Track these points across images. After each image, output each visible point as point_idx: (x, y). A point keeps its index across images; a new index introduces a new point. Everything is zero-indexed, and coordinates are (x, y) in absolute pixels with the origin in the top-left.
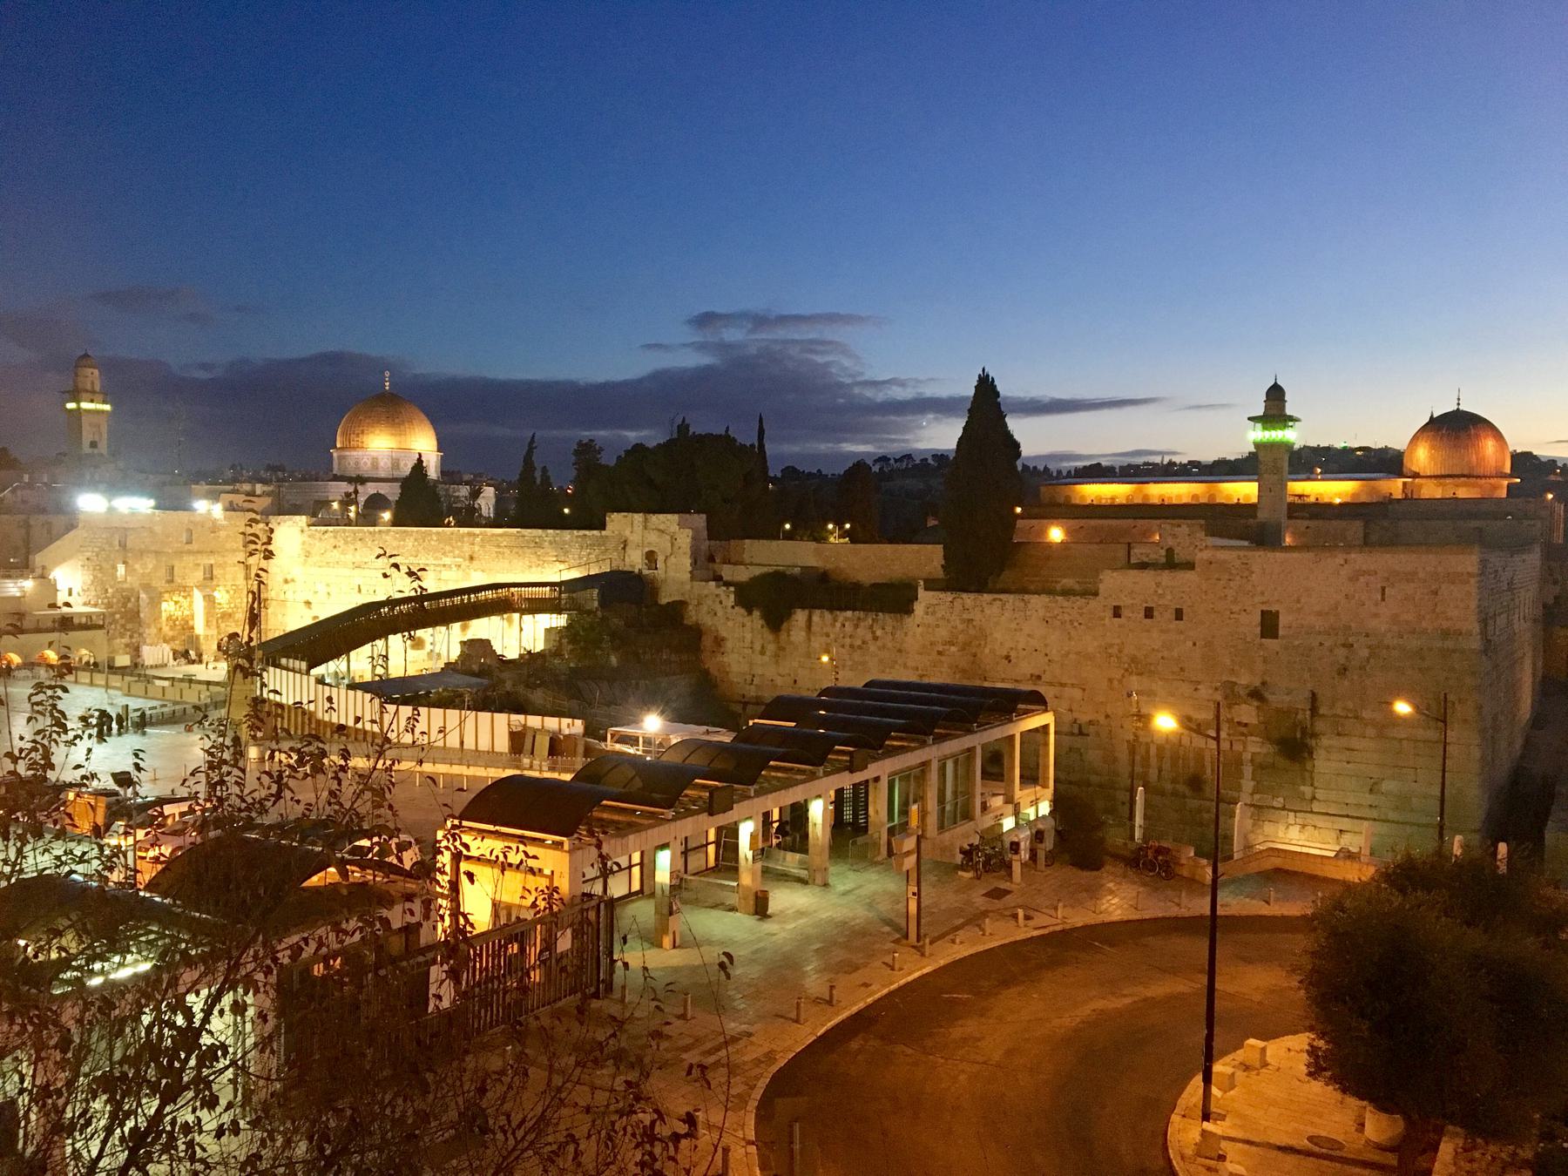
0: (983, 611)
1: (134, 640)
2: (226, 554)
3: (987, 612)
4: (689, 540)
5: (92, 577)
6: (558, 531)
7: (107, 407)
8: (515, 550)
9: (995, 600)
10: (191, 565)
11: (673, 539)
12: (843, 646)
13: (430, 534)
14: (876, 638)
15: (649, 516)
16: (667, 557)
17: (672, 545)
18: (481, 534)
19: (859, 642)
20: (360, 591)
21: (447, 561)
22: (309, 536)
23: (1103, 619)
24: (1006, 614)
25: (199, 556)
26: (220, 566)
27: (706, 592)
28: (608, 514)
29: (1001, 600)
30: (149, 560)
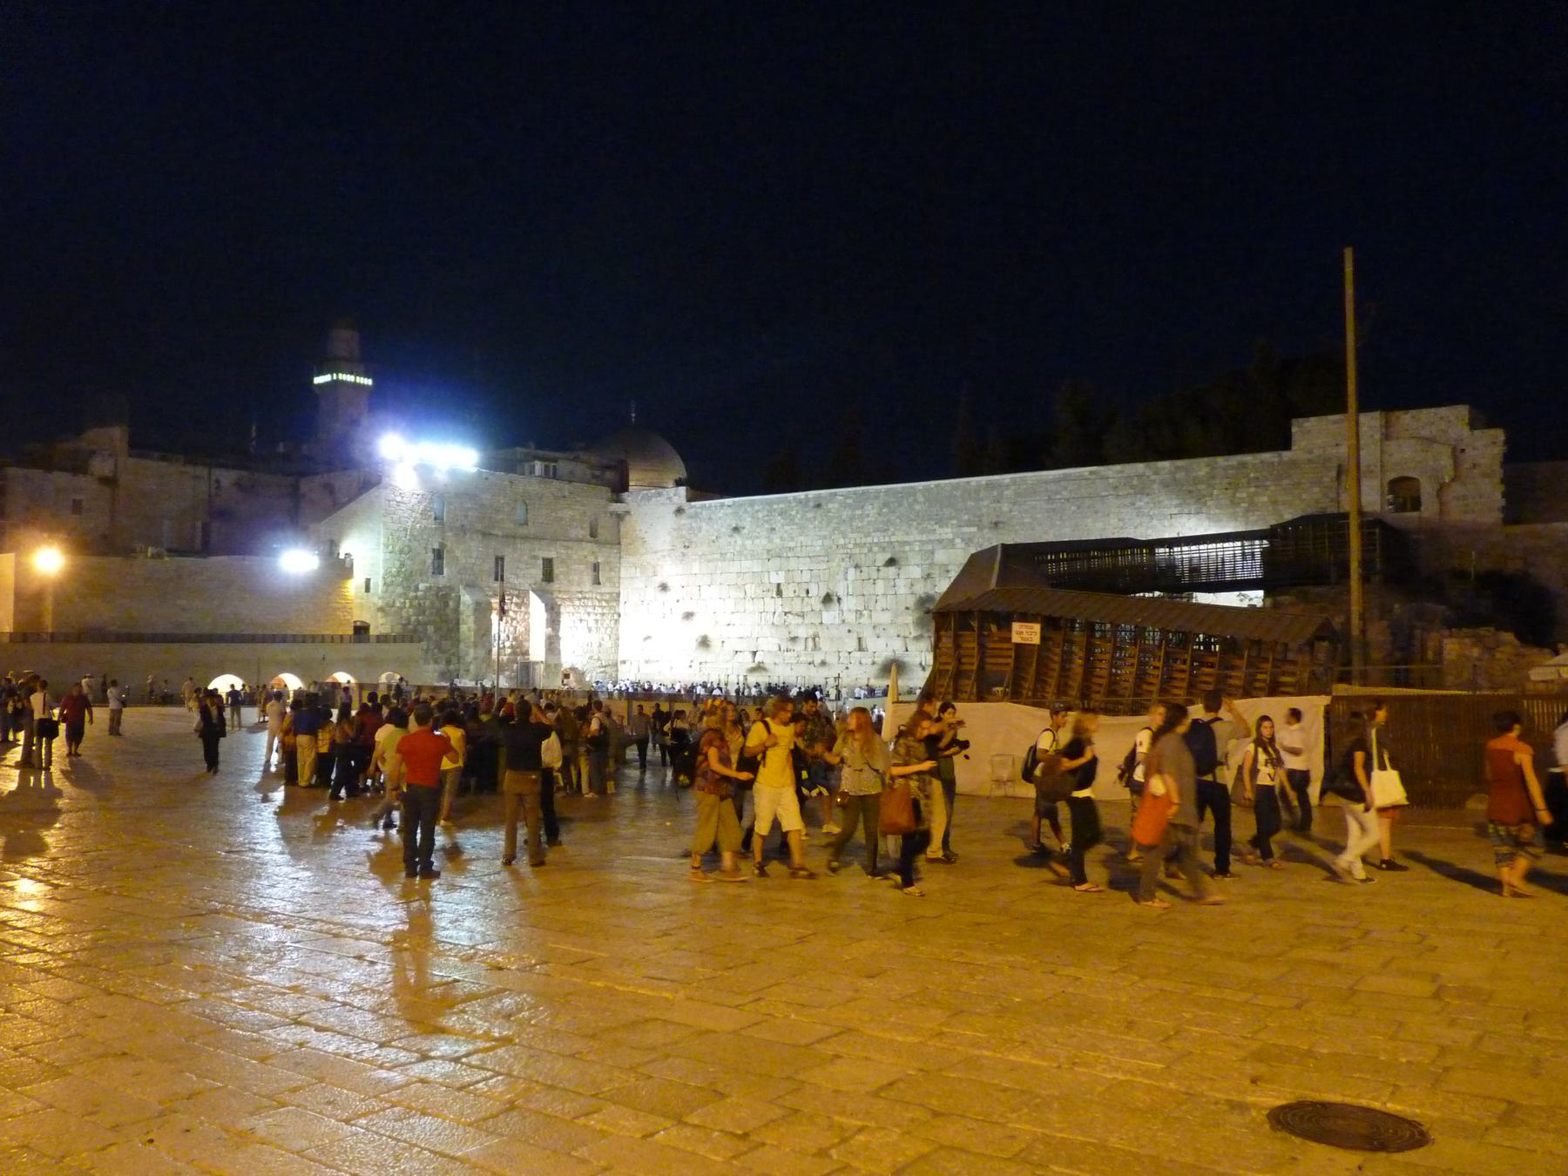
1: (451, 667)
2: (570, 544)
4: (1498, 450)
5: (397, 564)
6: (1180, 463)
7: (368, 382)
8: (1088, 502)
10: (526, 557)
11: (1457, 453)
13: (913, 493)
16: (1441, 489)
17: (1457, 464)
18: (1014, 482)
20: (779, 593)
21: (947, 533)
22: (691, 517)
25: (536, 545)
26: (562, 561)
28: (1294, 421)
30: (473, 544)
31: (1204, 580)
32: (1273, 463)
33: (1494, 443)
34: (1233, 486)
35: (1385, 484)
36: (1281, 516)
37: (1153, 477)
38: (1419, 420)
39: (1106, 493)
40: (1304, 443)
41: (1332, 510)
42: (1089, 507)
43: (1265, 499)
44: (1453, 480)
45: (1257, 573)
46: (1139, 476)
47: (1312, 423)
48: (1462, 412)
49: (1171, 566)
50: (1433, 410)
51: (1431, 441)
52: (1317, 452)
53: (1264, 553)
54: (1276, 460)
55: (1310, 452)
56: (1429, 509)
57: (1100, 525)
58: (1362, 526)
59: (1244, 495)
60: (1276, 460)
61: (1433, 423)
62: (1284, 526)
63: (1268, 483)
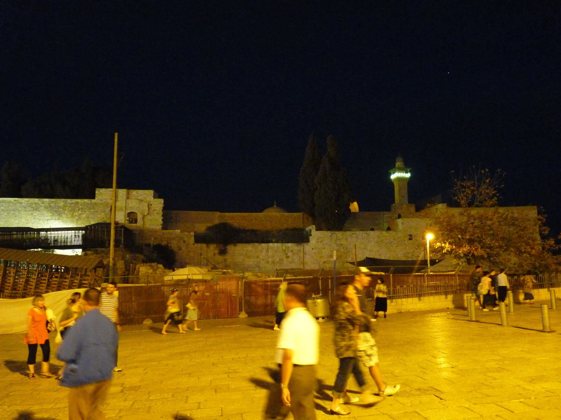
0: (347, 240)
3: (349, 240)
4: (161, 206)
6: (53, 200)
8: (12, 212)
9: (353, 234)
11: (149, 206)
12: (268, 262)
14: (288, 257)
15: (129, 190)
16: (144, 217)
19: (278, 260)
23: (405, 241)
24: (359, 241)
27: (173, 236)
28: (97, 189)
29: (356, 234)
31: (59, 244)
32: (88, 203)
33: (160, 203)
34: (73, 210)
35: (126, 214)
36: (90, 223)
37: (41, 204)
38: (138, 194)
39: (21, 209)
40: (100, 197)
41: (108, 221)
42: (12, 214)
43: (85, 216)
44: (148, 214)
45: (80, 243)
46: (36, 204)
47: (103, 190)
48: (150, 193)
49: (46, 239)
50: (142, 191)
51: (141, 201)
52: (104, 201)
53: (83, 235)
54: (90, 202)
55: (101, 201)
56: (140, 223)
57: (17, 221)
58: (116, 228)
59: (77, 214)
60: (90, 202)
61: (142, 195)
62: (91, 226)
63: (86, 210)
